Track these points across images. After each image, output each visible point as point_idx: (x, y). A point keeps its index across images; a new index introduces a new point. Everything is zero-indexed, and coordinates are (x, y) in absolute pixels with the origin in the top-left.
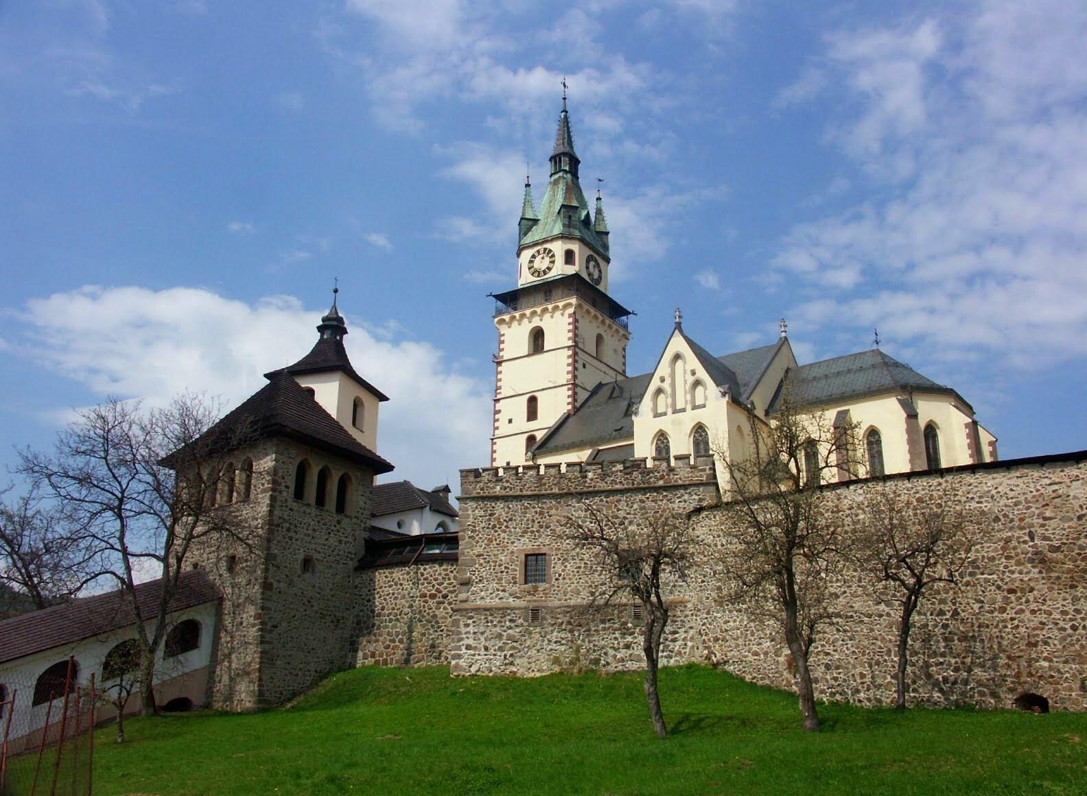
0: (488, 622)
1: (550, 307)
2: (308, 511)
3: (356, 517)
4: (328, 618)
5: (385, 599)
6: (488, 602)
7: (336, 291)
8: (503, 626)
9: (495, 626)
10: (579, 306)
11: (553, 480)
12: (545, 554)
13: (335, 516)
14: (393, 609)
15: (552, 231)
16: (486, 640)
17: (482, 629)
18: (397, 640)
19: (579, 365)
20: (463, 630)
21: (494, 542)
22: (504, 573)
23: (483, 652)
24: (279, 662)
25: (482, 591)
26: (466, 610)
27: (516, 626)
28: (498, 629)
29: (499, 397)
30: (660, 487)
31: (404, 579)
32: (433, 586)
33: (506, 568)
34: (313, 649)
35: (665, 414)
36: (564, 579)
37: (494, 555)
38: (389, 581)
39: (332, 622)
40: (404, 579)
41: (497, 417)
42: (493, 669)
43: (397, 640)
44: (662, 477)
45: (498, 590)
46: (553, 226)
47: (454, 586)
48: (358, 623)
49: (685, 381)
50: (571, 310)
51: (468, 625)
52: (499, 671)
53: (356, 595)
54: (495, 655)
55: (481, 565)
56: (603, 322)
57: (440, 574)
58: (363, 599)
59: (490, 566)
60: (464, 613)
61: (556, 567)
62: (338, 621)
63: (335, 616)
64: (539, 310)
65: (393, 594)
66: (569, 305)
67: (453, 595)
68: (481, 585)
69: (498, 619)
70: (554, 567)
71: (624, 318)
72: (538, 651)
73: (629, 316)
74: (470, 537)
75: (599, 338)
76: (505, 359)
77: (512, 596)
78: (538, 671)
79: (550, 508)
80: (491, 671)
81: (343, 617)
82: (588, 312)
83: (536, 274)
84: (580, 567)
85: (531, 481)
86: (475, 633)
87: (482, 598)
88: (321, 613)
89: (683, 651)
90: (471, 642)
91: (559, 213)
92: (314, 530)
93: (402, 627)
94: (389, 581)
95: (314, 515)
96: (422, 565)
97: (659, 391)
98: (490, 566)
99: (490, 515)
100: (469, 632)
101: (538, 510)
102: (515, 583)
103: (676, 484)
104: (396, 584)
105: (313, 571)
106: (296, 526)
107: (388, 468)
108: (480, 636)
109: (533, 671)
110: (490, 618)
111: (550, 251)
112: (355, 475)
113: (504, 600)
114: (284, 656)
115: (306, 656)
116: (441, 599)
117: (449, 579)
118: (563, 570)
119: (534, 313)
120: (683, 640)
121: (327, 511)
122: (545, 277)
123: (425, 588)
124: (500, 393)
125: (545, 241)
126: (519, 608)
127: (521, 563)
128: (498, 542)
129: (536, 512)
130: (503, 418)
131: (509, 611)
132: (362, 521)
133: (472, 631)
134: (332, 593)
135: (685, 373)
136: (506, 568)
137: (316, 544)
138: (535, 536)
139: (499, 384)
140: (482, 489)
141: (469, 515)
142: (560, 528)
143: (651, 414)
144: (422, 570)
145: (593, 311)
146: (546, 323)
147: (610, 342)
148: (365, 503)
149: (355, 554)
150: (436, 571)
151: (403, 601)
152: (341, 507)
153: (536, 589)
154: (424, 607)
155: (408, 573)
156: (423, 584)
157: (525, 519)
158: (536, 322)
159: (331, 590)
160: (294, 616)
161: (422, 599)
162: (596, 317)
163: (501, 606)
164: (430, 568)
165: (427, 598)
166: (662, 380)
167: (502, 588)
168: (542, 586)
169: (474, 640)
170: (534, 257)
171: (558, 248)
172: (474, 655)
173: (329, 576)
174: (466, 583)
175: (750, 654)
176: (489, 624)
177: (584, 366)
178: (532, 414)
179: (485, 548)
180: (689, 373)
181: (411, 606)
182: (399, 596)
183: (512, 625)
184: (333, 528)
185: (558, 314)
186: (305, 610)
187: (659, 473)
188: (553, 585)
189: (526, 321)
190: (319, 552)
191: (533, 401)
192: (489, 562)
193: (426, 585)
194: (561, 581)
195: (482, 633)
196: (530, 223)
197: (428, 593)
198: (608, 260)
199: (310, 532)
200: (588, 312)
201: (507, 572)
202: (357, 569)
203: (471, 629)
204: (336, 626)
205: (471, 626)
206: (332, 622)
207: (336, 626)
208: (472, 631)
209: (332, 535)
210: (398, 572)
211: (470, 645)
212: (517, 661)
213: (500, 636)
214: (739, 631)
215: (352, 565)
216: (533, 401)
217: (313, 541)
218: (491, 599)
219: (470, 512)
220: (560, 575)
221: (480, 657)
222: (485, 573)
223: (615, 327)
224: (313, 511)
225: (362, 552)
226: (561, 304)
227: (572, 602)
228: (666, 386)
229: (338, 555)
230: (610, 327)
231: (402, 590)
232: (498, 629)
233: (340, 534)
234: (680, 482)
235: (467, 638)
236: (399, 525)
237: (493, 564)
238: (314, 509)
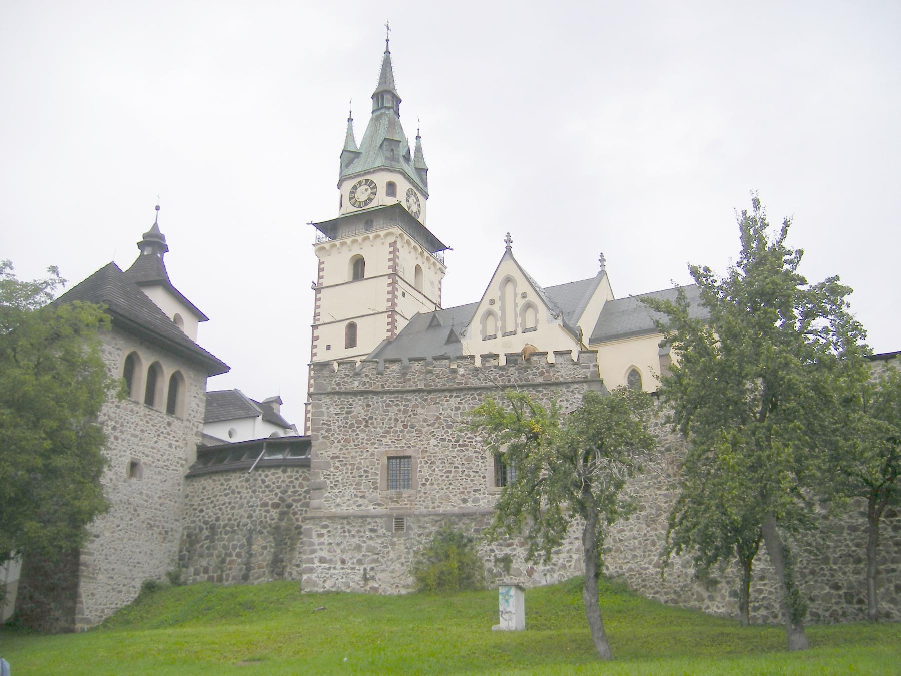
0: (344, 532)
1: (371, 236)
2: (136, 409)
3: (188, 420)
4: (155, 529)
5: (220, 509)
6: (344, 510)
7: (157, 208)
8: (362, 537)
9: (353, 536)
10: (401, 235)
11: (419, 376)
12: (410, 457)
13: (165, 416)
14: (230, 520)
15: (374, 163)
16: (342, 551)
17: (338, 540)
18: (234, 554)
19: (399, 294)
20: (316, 540)
21: (352, 443)
22: (364, 478)
23: (339, 565)
24: (100, 577)
25: (337, 496)
26: (320, 518)
27: (378, 536)
28: (356, 540)
29: (317, 323)
30: (539, 385)
31: (242, 487)
32: (276, 494)
33: (365, 471)
34: (139, 563)
35: (495, 337)
36: (432, 484)
37: (352, 457)
38: (225, 489)
39: (160, 533)
40: (242, 487)
41: (315, 343)
42: (352, 584)
43: (234, 554)
44: (542, 374)
45: (356, 496)
46: (375, 159)
47: (300, 495)
48: (189, 536)
49: (516, 305)
51: (321, 535)
52: (358, 587)
53: (186, 504)
54: (353, 569)
55: (337, 468)
56: (422, 254)
57: (283, 481)
58: (195, 509)
59: (347, 469)
60: (318, 521)
61: (422, 471)
62: (166, 532)
63: (163, 527)
64: (360, 239)
65: (230, 503)
67: (299, 505)
68: (337, 491)
69: (357, 529)
70: (420, 471)
71: (441, 252)
72: (403, 564)
73: (446, 251)
74: (324, 437)
75: (418, 269)
77: (374, 501)
78: (404, 587)
79: (416, 406)
80: (349, 587)
81: (172, 529)
82: (408, 242)
84: (450, 472)
85: (394, 377)
86: (330, 544)
87: (338, 505)
88: (148, 524)
89: (567, 565)
90: (325, 554)
91: (381, 146)
92: (142, 431)
93: (240, 539)
94: (225, 489)
95: (142, 414)
96: (263, 471)
97: (489, 313)
98: (347, 469)
99: (348, 413)
100: (323, 543)
101: (402, 408)
102: (376, 488)
103: (557, 381)
104: (233, 492)
105: (141, 476)
106: (122, 425)
107: (220, 368)
108: (335, 548)
109: (397, 587)
110: (347, 527)
111: (372, 182)
112: (188, 375)
113: (363, 508)
114: (106, 570)
115: (130, 571)
116: (286, 509)
117: (294, 487)
118: (431, 475)
119: (355, 241)
120: (568, 552)
121: (157, 411)
123: (266, 496)
125: (368, 172)
126: (381, 517)
127: (382, 466)
128: (356, 443)
129: (400, 410)
130: (321, 344)
131: (369, 520)
132: (193, 425)
133: (326, 542)
134: (160, 501)
135: (515, 295)
136: (365, 471)
137: (144, 446)
138: (399, 436)
139: (318, 311)
140: (338, 384)
141: (323, 413)
142: (427, 428)
143: (481, 337)
144: (263, 477)
145: (413, 243)
146: (367, 253)
147: (428, 273)
148: (198, 405)
149: (186, 460)
150: (280, 477)
151: (242, 512)
152: (171, 408)
153: (400, 495)
154: (266, 517)
155: (247, 480)
156: (264, 492)
157: (388, 418)
158: (356, 251)
159: (160, 498)
160: (118, 526)
161: (264, 509)
162: (415, 248)
163: (360, 514)
164: (273, 474)
165: (269, 508)
166: (492, 302)
167: (361, 495)
168: (406, 493)
169: (329, 551)
170: (355, 187)
171: (381, 180)
172: (329, 569)
173: (158, 482)
174: (320, 488)
175: (651, 567)
176: (347, 534)
177: (404, 295)
178: (351, 342)
179: (341, 449)
180: (519, 296)
181: (250, 516)
182: (237, 506)
183: (373, 535)
184: (162, 429)
185: (379, 241)
186: (131, 520)
187: (538, 369)
188: (420, 491)
189: (345, 249)
190: (147, 456)
191: (352, 329)
192: (346, 464)
193: (267, 493)
194: (428, 486)
195: (338, 544)
196: (353, 155)
197: (270, 502)
198: (427, 196)
199: (137, 433)
200: (408, 242)
201: (367, 476)
202: (188, 477)
203: (326, 540)
204: (164, 538)
205: (326, 537)
206: (160, 533)
207: (164, 538)
208: (326, 542)
209: (161, 438)
210: (235, 479)
211: (325, 558)
212: (379, 576)
213: (358, 548)
214: (636, 542)
215: (184, 471)
216: (352, 329)
217: (140, 443)
218: (348, 506)
219: (324, 409)
220: (427, 480)
221: (336, 572)
222: (341, 478)
223: (433, 260)
224: (142, 409)
225: (193, 458)
226: (382, 233)
227: (441, 510)
228: (496, 308)
229: (168, 460)
230: (428, 259)
231: (241, 498)
232: (356, 540)
233: (170, 437)
234: (561, 379)
235: (321, 549)
236: (230, 435)
237: (350, 467)
238: (142, 408)
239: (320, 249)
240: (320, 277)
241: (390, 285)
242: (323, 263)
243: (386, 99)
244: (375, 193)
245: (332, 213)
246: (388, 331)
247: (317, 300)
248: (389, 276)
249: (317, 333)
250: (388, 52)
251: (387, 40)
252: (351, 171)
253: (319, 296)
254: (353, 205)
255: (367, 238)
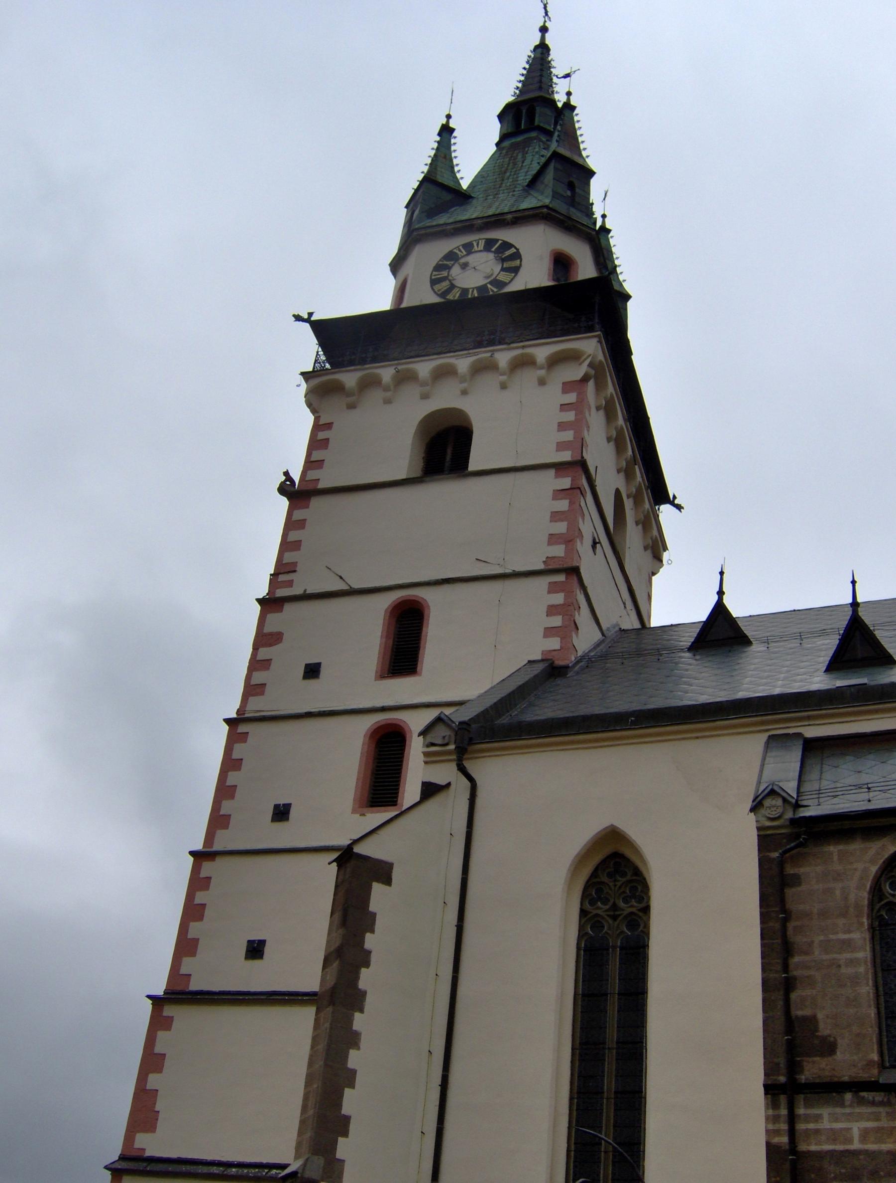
29: (281, 593)
41: (264, 653)
50: (576, 372)
66: (573, 357)
76: (321, 485)
111: (507, 245)
119: (444, 373)
124: (290, 584)
125: (498, 221)
130: (288, 660)
158: (446, 398)
170: (451, 256)
185: (529, 377)
189: (411, 392)
239: (320, 389)
240: (310, 464)
241: (559, 494)
242: (329, 426)
245: (376, 295)
246: (549, 632)
247: (291, 524)
248: (560, 467)
249: (275, 621)
253: (298, 515)
255: (489, 367)
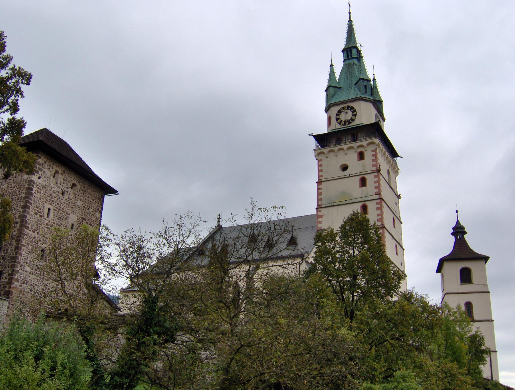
66: (373, 143)
83: (342, 123)
122: (351, 125)
170: (339, 111)
243: (352, 52)
244: (355, 115)
245: (324, 129)
250: (350, 21)
251: (350, 13)
252: (333, 101)
254: (340, 124)
